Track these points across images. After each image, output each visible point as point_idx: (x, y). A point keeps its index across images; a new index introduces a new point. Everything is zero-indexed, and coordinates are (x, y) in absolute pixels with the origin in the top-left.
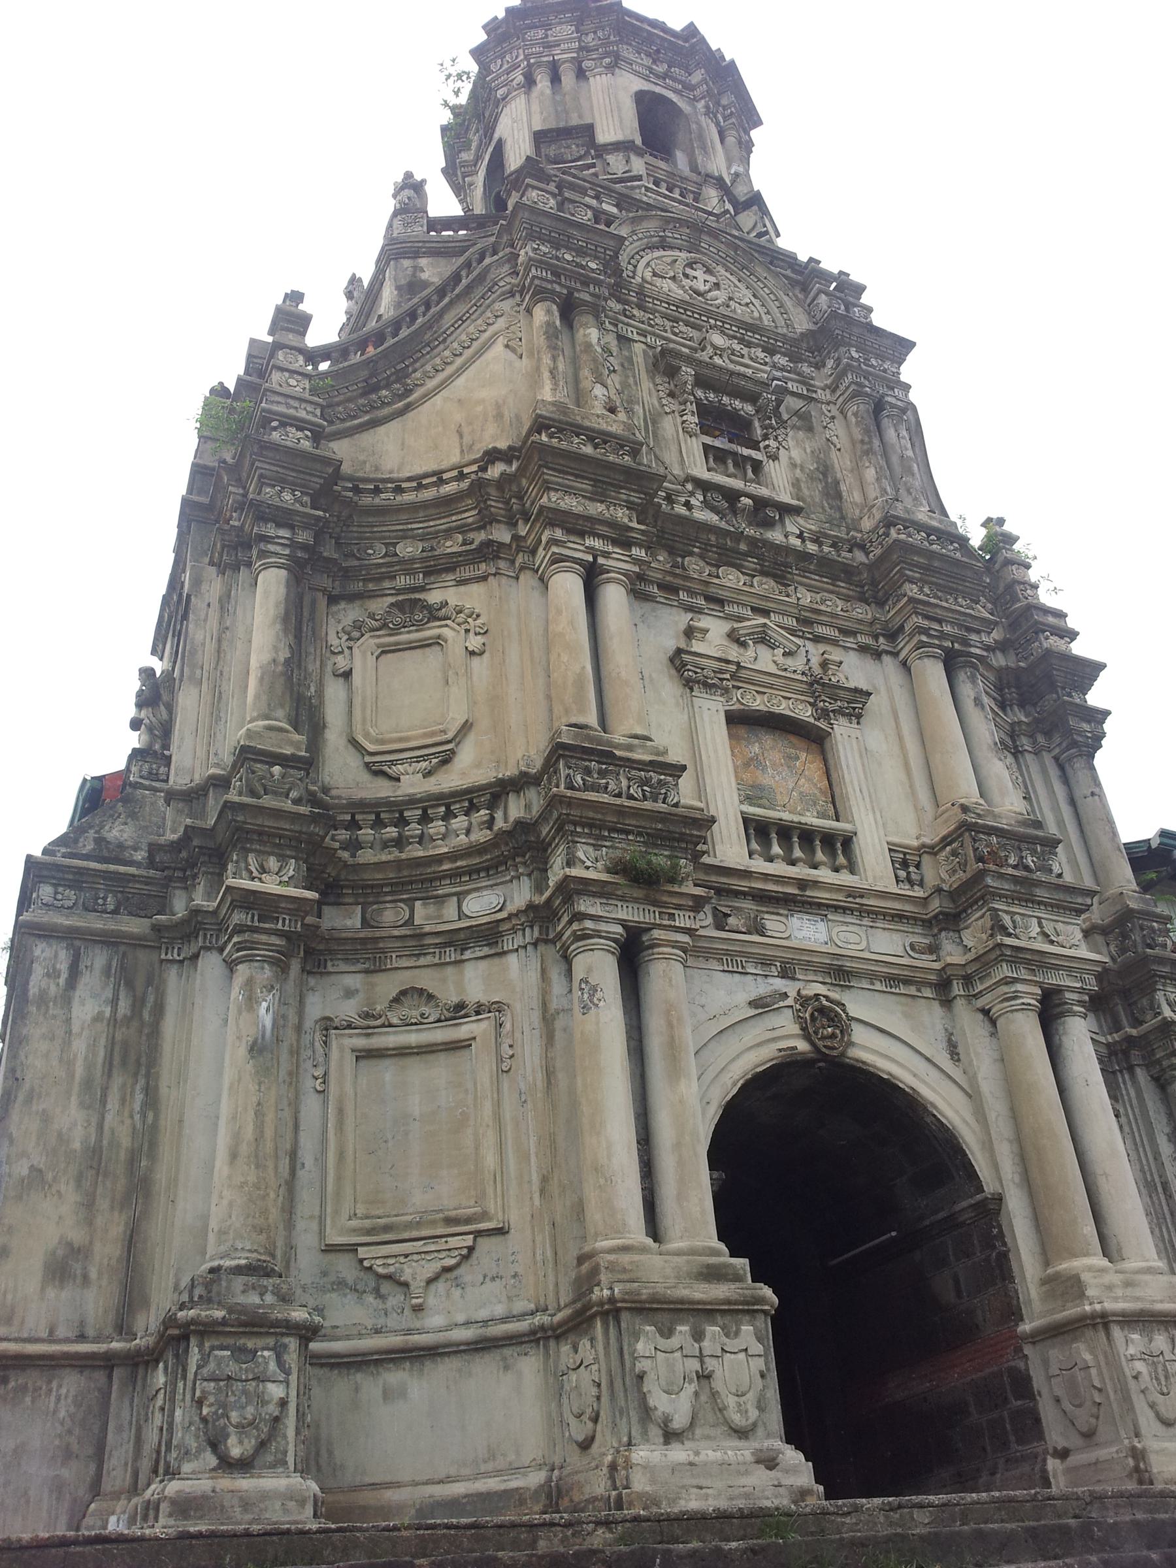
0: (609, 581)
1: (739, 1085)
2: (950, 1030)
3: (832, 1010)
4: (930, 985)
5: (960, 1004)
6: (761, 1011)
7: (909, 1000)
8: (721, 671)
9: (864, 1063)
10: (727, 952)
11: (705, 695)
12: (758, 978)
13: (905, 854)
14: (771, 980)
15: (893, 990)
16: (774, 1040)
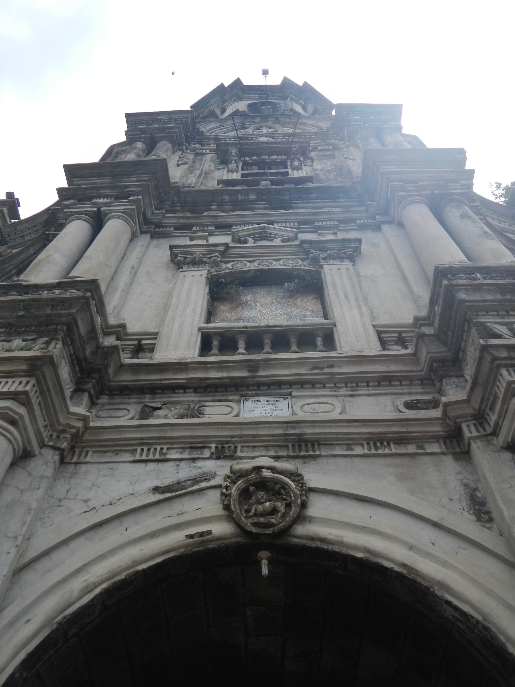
0: (109, 219)
1: (98, 591)
2: (472, 484)
3: (276, 481)
4: (436, 439)
5: (476, 447)
6: (168, 495)
7: (406, 460)
8: (210, 253)
9: (323, 540)
10: (142, 442)
11: (193, 269)
12: (183, 464)
13: (400, 333)
14: (199, 464)
15: (380, 451)
16: (178, 527)
